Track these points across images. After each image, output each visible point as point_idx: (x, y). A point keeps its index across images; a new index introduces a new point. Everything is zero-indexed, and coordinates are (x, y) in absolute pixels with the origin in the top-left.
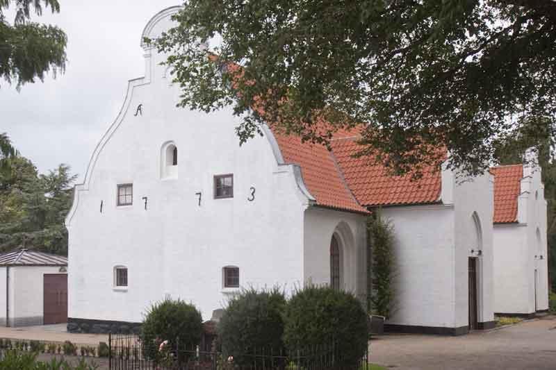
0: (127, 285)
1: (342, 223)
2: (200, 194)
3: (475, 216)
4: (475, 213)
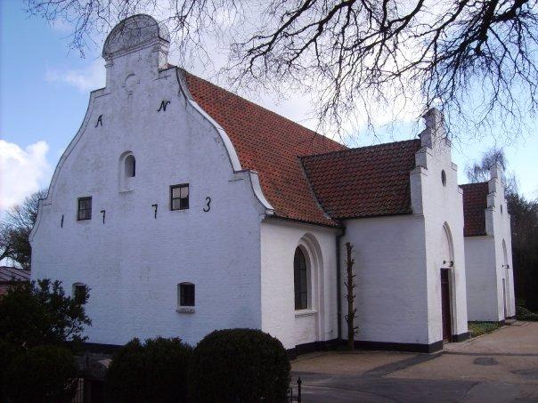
0: (194, 305)
1: (306, 235)
2: (156, 205)
3: (446, 227)
4: (445, 223)
